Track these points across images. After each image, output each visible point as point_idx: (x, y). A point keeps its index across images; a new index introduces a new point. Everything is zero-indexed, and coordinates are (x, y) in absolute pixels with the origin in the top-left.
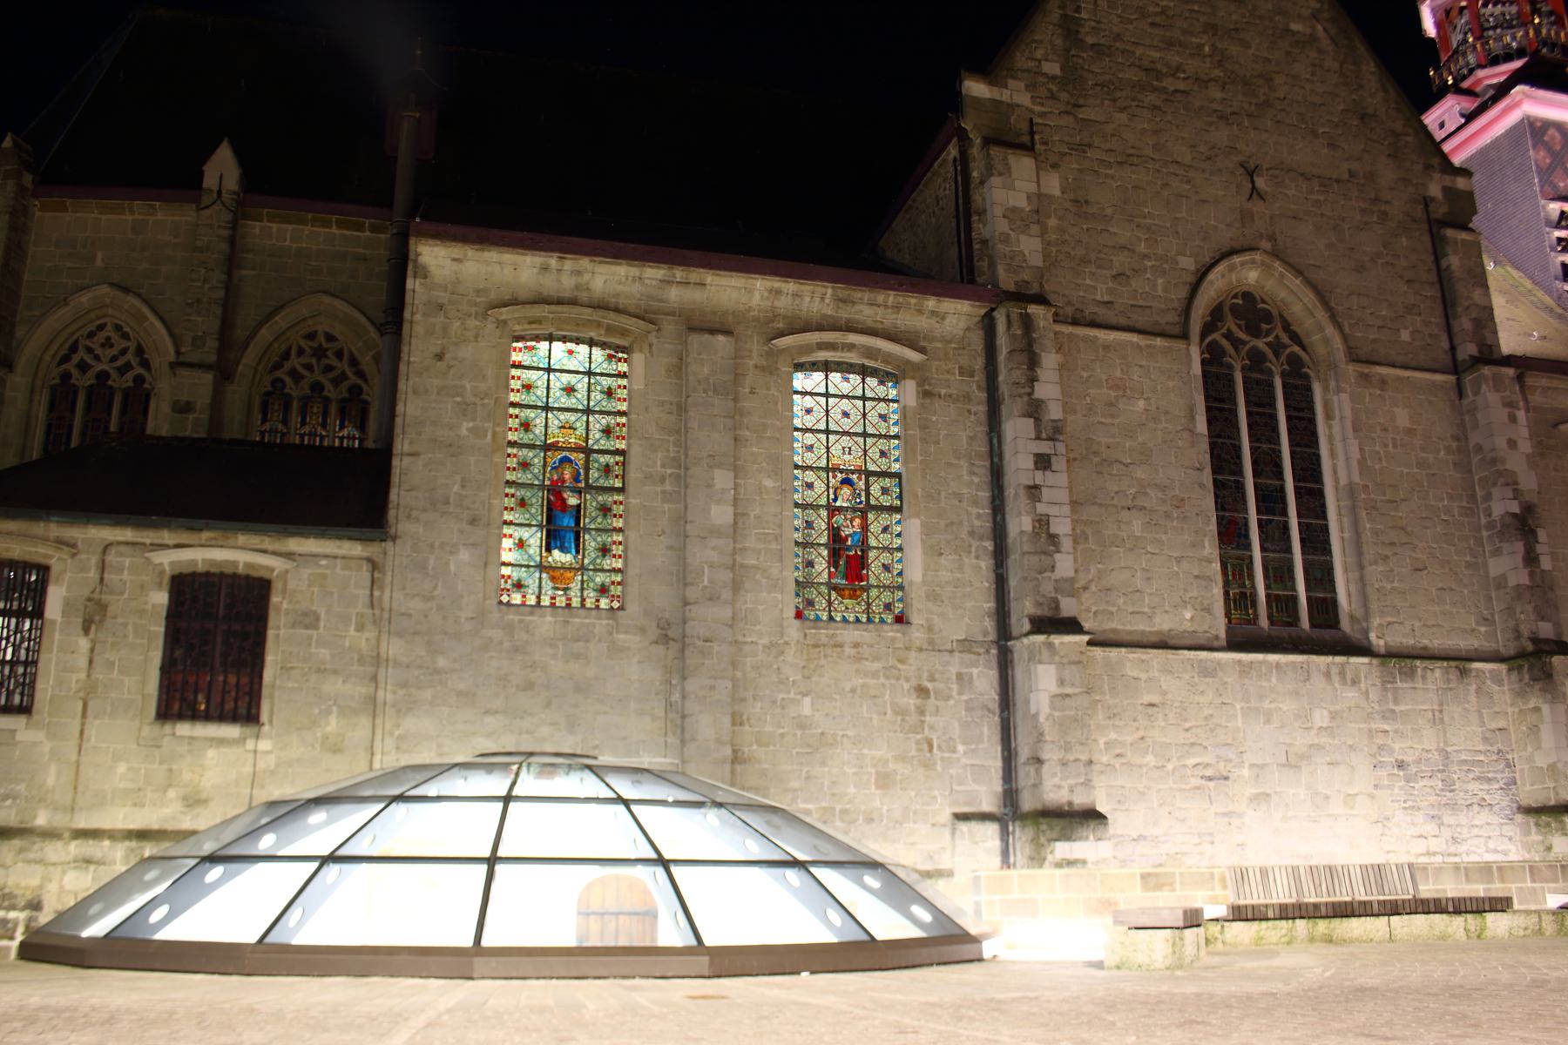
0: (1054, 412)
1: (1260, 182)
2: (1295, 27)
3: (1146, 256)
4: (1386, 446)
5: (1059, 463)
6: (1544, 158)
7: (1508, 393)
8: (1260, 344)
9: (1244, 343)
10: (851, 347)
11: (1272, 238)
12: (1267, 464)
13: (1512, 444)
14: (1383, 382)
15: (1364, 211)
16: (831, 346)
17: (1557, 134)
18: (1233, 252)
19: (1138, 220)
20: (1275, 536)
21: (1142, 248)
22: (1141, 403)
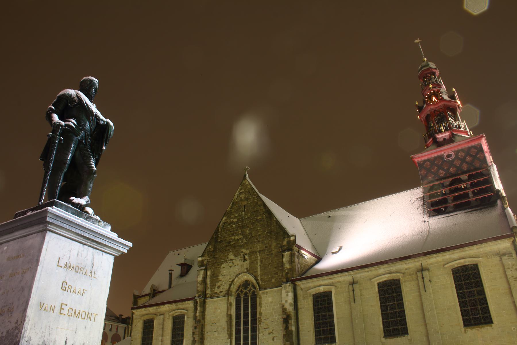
0: (198, 318)
2: (259, 218)
3: (223, 281)
4: (266, 307)
5: (198, 327)
6: (424, 172)
7: (287, 289)
8: (246, 291)
9: (243, 291)
10: (179, 312)
12: (246, 315)
13: (286, 301)
14: (267, 293)
15: (267, 255)
16: (176, 313)
17: (428, 163)
18: (240, 274)
19: (223, 274)
20: (246, 330)
21: (223, 280)
22: (219, 311)
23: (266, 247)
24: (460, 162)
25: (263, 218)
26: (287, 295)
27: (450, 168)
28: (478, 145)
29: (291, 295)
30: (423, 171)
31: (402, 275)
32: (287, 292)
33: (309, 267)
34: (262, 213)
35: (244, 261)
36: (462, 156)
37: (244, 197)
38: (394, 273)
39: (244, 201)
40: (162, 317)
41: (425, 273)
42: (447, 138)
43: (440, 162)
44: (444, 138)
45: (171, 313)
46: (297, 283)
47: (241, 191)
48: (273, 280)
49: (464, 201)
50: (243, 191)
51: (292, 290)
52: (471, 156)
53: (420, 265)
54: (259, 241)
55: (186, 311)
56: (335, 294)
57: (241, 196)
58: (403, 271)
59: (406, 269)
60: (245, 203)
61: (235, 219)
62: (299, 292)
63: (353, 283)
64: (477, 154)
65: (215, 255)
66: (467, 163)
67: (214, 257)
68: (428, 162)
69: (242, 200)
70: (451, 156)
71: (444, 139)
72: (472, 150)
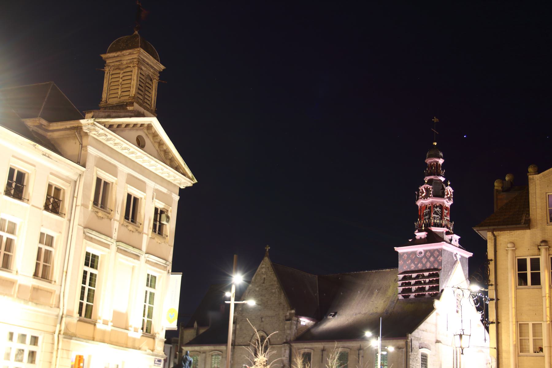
1: (263, 319)
2: (273, 291)
10: (216, 353)
11: (263, 328)
14: (274, 347)
16: (214, 353)
17: (406, 255)
21: (247, 333)
23: (276, 315)
24: (426, 260)
25: (275, 292)
26: (285, 352)
27: (419, 263)
28: (440, 249)
29: (288, 352)
30: (401, 261)
31: (349, 350)
32: (285, 350)
33: (302, 332)
34: (275, 288)
35: (261, 322)
36: (428, 255)
37: (265, 272)
38: (346, 348)
39: (264, 275)
40: (204, 354)
41: (361, 351)
42: (423, 237)
43: (414, 257)
44: (420, 236)
45: (211, 353)
46: (293, 344)
47: (263, 266)
48: (279, 339)
49: (420, 293)
50: (264, 266)
51: (289, 348)
52: (434, 257)
53: (360, 346)
54: (272, 309)
55: (221, 353)
56: (313, 355)
57: (262, 270)
58: (350, 348)
59: (352, 347)
60: (265, 276)
61: (257, 288)
62: (294, 350)
63: (323, 350)
64: (438, 257)
65: (242, 314)
66: (430, 262)
67: (241, 315)
68: (407, 255)
69: (263, 274)
70: (421, 254)
71: (421, 238)
72: (435, 252)
